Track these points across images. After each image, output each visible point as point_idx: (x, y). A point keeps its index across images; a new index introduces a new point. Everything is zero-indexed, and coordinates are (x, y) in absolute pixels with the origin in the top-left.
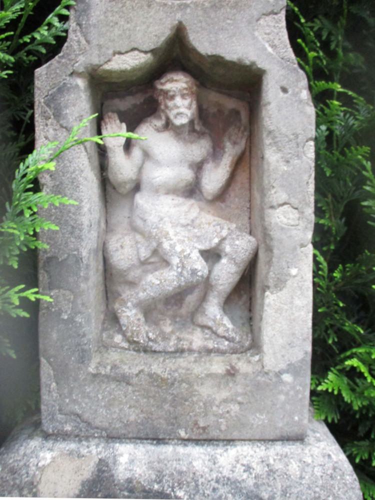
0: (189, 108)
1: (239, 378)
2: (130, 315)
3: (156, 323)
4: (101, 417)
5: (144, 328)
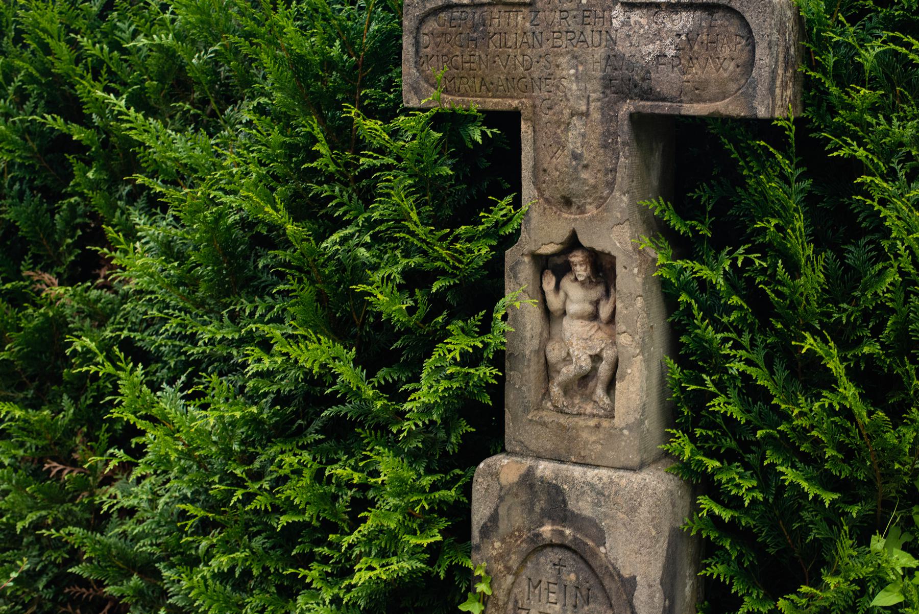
0: (585, 270)
1: (601, 429)
2: (555, 390)
3: (572, 398)
4: (533, 445)
5: (562, 399)
